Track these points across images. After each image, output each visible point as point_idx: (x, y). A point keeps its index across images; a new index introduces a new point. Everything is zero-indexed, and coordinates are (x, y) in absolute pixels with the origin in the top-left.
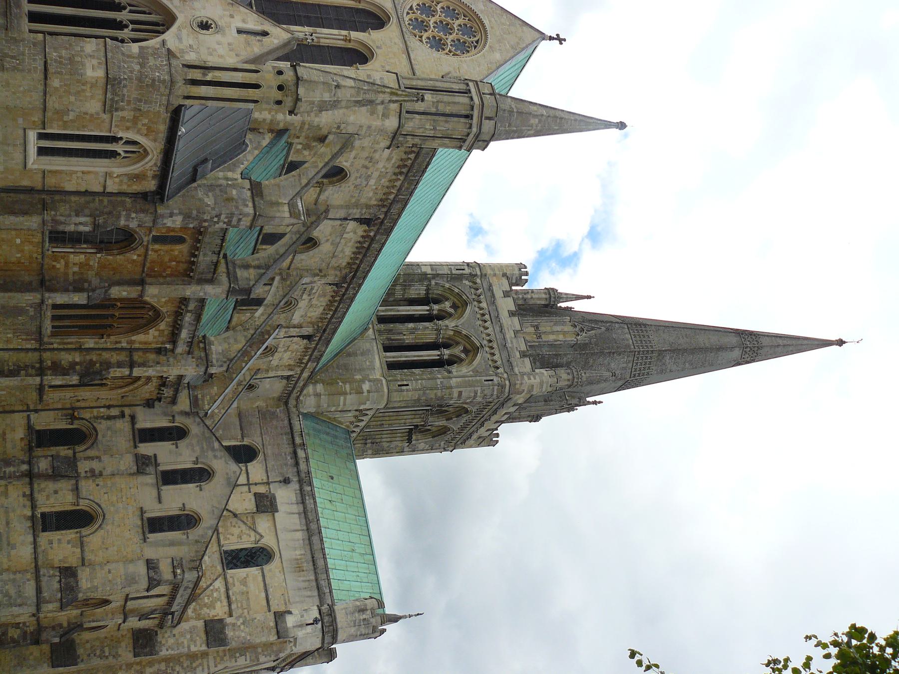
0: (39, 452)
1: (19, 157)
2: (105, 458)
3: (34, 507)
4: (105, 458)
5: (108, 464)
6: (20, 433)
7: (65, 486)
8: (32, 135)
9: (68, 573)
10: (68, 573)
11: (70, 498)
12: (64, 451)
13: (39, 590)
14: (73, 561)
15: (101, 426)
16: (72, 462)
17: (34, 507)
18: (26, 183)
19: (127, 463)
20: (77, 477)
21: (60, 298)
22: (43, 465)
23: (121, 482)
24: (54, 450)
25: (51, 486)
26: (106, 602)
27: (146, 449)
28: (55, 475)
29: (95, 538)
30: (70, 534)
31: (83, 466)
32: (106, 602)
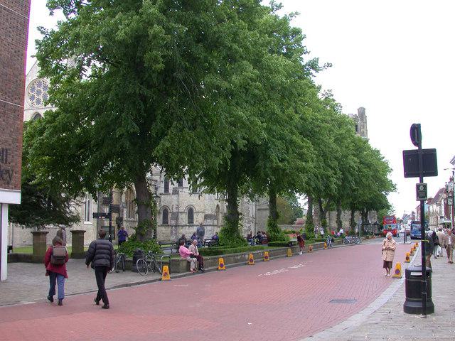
0: (169, 223)
1: (89, 227)
2: (173, 203)
3: (186, 226)
4: (173, 203)
5: (175, 203)
6: (163, 229)
7: (180, 216)
8: (85, 223)
9: (206, 217)
10: (206, 217)
11: (184, 215)
12: (170, 216)
13: (210, 225)
14: (203, 215)
15: (163, 204)
16: (173, 213)
17: (186, 226)
18: (96, 225)
19: (175, 197)
20: (178, 213)
21: (125, 216)
22: (173, 222)
23: (181, 199)
24: (169, 219)
25: (180, 220)
26: (218, 206)
27: (171, 191)
28: (177, 219)
29: (197, 208)
30: (195, 215)
31: (175, 210)
32: (218, 206)
